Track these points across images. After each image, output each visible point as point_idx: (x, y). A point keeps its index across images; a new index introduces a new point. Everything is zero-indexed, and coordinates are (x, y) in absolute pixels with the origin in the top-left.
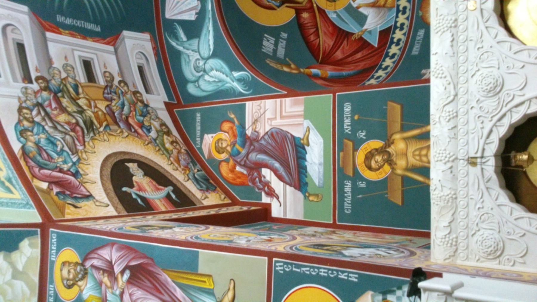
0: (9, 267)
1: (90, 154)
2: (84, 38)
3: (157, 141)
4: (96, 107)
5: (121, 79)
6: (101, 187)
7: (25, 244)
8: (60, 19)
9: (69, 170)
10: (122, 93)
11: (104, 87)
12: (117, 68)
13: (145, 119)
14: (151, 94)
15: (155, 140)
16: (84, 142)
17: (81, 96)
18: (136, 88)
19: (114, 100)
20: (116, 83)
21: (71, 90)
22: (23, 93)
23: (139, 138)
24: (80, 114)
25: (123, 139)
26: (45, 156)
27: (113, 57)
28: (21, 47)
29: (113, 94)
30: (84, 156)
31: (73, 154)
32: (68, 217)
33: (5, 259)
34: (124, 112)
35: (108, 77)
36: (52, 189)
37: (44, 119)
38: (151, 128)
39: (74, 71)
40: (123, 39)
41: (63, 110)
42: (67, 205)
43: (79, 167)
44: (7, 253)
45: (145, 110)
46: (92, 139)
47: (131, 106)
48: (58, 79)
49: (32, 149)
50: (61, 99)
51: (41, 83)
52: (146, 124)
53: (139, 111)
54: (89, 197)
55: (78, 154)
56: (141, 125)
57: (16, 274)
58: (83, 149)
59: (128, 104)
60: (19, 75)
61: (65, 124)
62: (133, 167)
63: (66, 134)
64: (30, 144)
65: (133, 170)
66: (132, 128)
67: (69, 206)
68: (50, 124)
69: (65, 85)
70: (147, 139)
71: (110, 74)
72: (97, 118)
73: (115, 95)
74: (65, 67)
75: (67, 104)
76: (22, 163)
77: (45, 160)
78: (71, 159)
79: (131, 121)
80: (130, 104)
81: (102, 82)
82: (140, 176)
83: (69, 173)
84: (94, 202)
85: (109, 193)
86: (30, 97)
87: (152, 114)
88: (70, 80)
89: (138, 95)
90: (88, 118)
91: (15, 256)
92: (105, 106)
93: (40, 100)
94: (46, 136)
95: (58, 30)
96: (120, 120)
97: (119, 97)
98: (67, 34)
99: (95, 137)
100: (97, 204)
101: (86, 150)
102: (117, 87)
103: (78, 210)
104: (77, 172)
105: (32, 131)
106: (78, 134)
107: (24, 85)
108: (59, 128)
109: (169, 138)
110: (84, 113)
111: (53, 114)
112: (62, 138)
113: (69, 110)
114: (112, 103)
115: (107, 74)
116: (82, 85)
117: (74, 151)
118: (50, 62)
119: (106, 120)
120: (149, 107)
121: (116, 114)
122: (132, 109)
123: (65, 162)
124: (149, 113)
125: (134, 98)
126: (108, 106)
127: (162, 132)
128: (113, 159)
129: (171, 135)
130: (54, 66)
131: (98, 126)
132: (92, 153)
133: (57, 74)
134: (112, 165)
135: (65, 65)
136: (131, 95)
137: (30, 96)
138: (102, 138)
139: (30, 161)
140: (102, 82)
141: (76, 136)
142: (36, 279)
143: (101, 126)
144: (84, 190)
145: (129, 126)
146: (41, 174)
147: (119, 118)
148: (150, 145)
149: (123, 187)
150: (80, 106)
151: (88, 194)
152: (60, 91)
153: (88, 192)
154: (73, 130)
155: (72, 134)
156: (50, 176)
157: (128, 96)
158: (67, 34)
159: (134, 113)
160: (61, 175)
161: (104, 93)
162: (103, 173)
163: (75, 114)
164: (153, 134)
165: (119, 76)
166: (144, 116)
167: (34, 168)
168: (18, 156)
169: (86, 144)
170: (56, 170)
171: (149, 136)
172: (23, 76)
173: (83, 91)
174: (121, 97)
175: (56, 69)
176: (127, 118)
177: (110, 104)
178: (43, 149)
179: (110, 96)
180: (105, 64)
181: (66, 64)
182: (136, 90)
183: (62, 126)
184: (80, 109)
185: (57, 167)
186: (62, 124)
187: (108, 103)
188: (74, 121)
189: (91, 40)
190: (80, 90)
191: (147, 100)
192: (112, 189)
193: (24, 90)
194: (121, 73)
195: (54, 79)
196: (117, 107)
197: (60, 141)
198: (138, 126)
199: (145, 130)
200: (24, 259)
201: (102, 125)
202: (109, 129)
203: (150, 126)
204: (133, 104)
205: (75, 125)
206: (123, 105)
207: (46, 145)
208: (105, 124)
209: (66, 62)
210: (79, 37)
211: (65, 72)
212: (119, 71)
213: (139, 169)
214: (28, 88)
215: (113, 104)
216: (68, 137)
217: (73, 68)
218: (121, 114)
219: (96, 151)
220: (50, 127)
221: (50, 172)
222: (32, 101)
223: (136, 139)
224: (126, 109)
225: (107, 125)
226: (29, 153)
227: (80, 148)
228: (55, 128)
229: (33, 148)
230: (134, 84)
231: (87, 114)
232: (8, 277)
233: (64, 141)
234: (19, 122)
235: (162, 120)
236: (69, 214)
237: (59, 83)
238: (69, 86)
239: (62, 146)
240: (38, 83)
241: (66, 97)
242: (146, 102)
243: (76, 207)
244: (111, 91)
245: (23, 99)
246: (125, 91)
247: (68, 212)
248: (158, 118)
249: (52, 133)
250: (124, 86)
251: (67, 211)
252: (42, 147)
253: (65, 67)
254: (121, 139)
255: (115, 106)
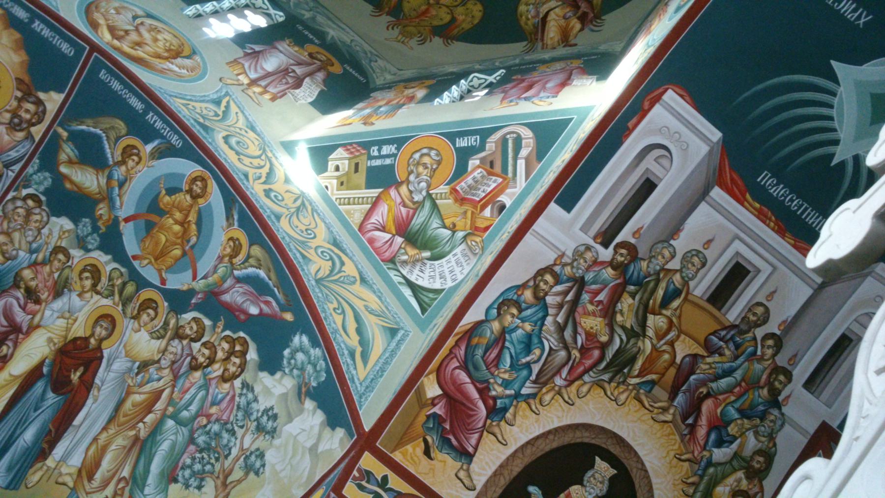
0: (316, 436)
1: (561, 400)
2: (781, 232)
3: (711, 470)
4: (671, 344)
5: (778, 332)
6: (504, 457)
7: (340, 432)
8: (765, 179)
9: (495, 399)
10: (754, 353)
11: (727, 324)
12: (793, 312)
13: (739, 422)
14: (812, 394)
15: (709, 464)
16: (580, 377)
17: (668, 313)
18: (795, 365)
19: (721, 355)
20: (760, 333)
21: (660, 293)
22: (576, 251)
23: (682, 441)
24: (627, 336)
25: (652, 422)
26: (493, 355)
27: (808, 292)
28: (648, 187)
29: (731, 345)
30: (547, 398)
31: (534, 382)
32: (397, 456)
33: (322, 424)
34: (714, 385)
35: (755, 314)
36: (434, 405)
37: (560, 306)
38: (731, 443)
39: (698, 270)
40: (866, 276)
41: (609, 312)
42: (422, 439)
43: (516, 407)
44: (326, 423)
45: (761, 408)
46: (599, 384)
47: (743, 384)
48: (658, 264)
49: (488, 333)
50: (625, 295)
51: (622, 255)
52: (732, 429)
53: (749, 402)
54: (466, 456)
55: (542, 388)
56: (719, 425)
57: (313, 449)
58: (560, 387)
59: (739, 378)
60: (598, 225)
61: (584, 336)
62: (602, 469)
63: (566, 347)
64: (496, 326)
65: (593, 476)
66: (694, 415)
67: (423, 445)
68: (560, 319)
69: (658, 281)
70: (696, 453)
71: (767, 310)
72: (651, 361)
73: (733, 348)
74: (690, 255)
75: (625, 310)
76: (451, 342)
77: (484, 361)
78: (522, 385)
79: (707, 406)
80: (743, 379)
81: (734, 313)
82: (590, 494)
83: (491, 402)
84: (462, 468)
85: (501, 474)
86: (579, 264)
87: (767, 423)
88: (677, 278)
89: (782, 378)
90: (635, 350)
91: (328, 430)
92: (690, 352)
93: (589, 277)
94: (533, 330)
95: (744, 196)
96: (688, 390)
97: (736, 358)
98: (754, 208)
99: (606, 385)
100: (462, 474)
101: (564, 391)
102: (755, 339)
103: (424, 459)
104: (505, 410)
105: (520, 311)
106: (584, 361)
107: (591, 242)
108: (568, 334)
109: (744, 482)
110: (638, 340)
111: (584, 308)
112: (551, 348)
113: (619, 318)
114: (708, 357)
115: (760, 310)
116: (690, 297)
117: (543, 380)
118: (675, 232)
119: (663, 375)
120: (780, 409)
121: (693, 377)
122: (737, 390)
123: (506, 384)
124: (762, 419)
125: (764, 377)
126: (695, 356)
127: (746, 465)
128: (587, 434)
129: (756, 482)
130: (672, 242)
131: (636, 373)
132: (567, 403)
133: (663, 257)
134: (572, 442)
135: (694, 253)
136: (765, 369)
137: (582, 261)
138: (616, 393)
139: (463, 348)
140: (734, 313)
141: (577, 360)
142: (318, 477)
143: (637, 376)
144: (473, 441)
145: (693, 409)
146: (452, 374)
147: (690, 386)
148: (686, 464)
149: (533, 484)
150: (643, 325)
151: (471, 450)
152: (639, 283)
153: (476, 449)
154: (584, 351)
155: (575, 353)
156: (459, 387)
157: (757, 367)
158: (754, 208)
159: (733, 398)
160: (475, 395)
161: (713, 334)
162: (540, 441)
163: (619, 331)
164: (720, 454)
165: (780, 325)
166: (744, 413)
167: (455, 360)
168: (457, 330)
169: (577, 383)
170: (478, 384)
171: (710, 451)
172: (603, 229)
173: (680, 307)
174: (741, 359)
175: (671, 249)
176: (708, 395)
177: (703, 357)
178: (504, 343)
179: (722, 343)
180: (774, 292)
181: (699, 252)
182: (789, 368)
183: (575, 332)
184: (637, 329)
185: (487, 381)
186: (579, 330)
187: (701, 351)
188: (604, 339)
189: (793, 242)
190: (676, 304)
191: (788, 397)
192: (515, 474)
193: (582, 248)
194: (790, 326)
195: (650, 262)
196: (711, 368)
197: (543, 350)
198: (709, 422)
199: (713, 436)
200: (327, 447)
201: (644, 376)
202: (648, 389)
203: (735, 438)
204: (751, 384)
205: (598, 345)
206: (728, 373)
207: (515, 342)
208: (654, 377)
209: (701, 249)
210: (772, 224)
211: (681, 263)
212: (789, 319)
213: (607, 482)
214: (593, 250)
215: (709, 360)
216: (563, 354)
217: (704, 265)
218: (703, 383)
219: (576, 404)
220: (556, 322)
221: (468, 380)
222: (574, 270)
223: (677, 437)
224: (724, 383)
225: (653, 383)
226: (476, 336)
227: (559, 381)
228: (561, 329)
229: (492, 332)
230: (795, 356)
231: (640, 344)
232: (309, 444)
233: (549, 354)
234: (524, 286)
235: (775, 445)
236: (404, 455)
237: (652, 272)
238: (663, 285)
239: (536, 359)
240: (616, 252)
241: (637, 297)
242: (780, 398)
243: (427, 452)
244: (732, 338)
245: (566, 260)
246: (763, 354)
247: (407, 450)
248: (771, 437)
249: (548, 332)
250: (769, 347)
251: (409, 448)
252: (505, 340)
253: (690, 255)
254: (648, 416)
255: (709, 364)
